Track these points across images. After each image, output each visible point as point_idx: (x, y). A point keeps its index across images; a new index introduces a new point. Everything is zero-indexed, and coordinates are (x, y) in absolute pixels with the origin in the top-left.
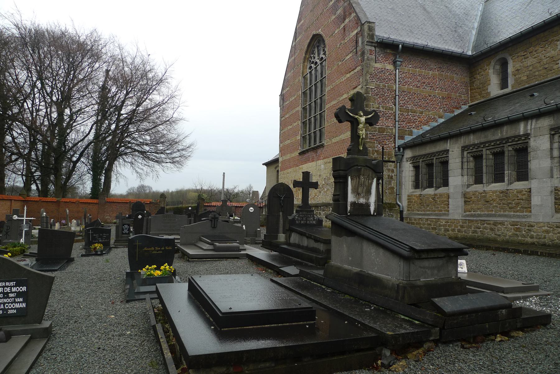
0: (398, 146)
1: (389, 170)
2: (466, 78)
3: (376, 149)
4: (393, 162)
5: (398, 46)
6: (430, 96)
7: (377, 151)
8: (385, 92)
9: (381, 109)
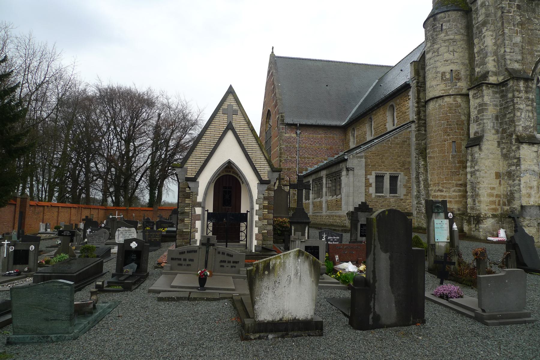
3: (286, 179)
5: (297, 124)
8: (291, 149)
9: (289, 158)
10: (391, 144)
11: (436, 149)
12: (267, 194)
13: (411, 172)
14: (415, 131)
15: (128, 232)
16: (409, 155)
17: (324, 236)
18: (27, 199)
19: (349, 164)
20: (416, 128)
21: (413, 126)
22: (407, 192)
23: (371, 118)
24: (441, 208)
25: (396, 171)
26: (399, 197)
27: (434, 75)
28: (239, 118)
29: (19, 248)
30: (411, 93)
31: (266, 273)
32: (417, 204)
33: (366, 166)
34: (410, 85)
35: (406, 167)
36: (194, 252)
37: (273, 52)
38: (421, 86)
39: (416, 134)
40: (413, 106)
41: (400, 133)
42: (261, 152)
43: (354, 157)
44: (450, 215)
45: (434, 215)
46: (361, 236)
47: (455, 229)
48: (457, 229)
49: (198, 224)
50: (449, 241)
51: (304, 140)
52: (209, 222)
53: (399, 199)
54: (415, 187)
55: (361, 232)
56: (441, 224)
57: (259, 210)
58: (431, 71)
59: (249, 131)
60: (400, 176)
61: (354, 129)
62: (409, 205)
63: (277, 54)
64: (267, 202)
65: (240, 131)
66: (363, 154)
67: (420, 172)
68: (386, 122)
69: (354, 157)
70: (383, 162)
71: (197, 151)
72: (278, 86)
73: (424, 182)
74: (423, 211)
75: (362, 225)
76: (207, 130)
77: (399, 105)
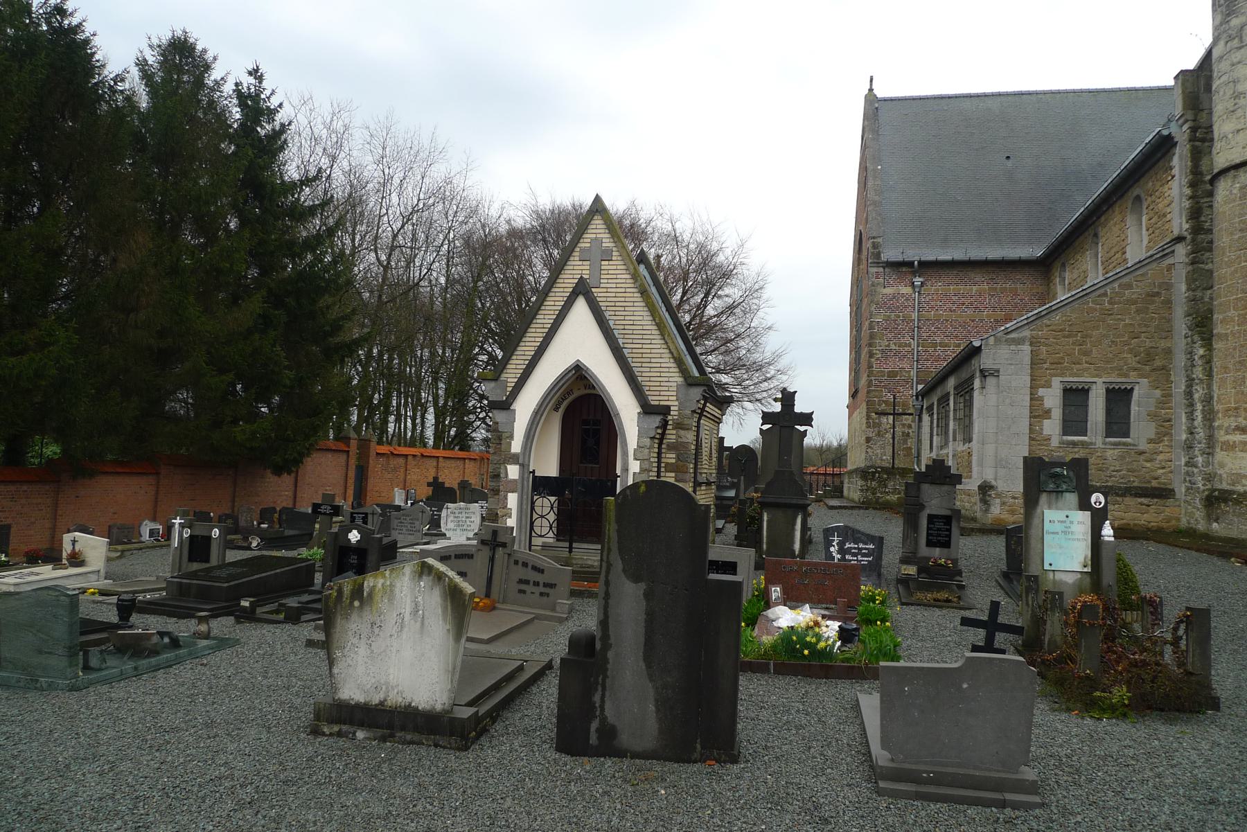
0: (917, 393)
1: (904, 425)
2: (1040, 287)
3: (884, 399)
4: (912, 414)
5: (913, 262)
6: (973, 321)
7: (886, 402)
8: (898, 325)
9: (893, 347)
10: (1110, 303)
11: (1233, 312)
12: (674, 437)
13: (1172, 378)
14: (1186, 264)
15: (464, 511)
16: (1168, 332)
17: (836, 540)
18: (370, 441)
19: (986, 360)
20: (1188, 255)
21: (1181, 251)
22: (1157, 433)
23: (1096, 235)
24: (1065, 480)
25: (1126, 376)
26: (1134, 445)
27: (1230, 105)
28: (615, 267)
29: (197, 533)
30: (1176, 161)
31: (356, 603)
32: (1187, 464)
33: (1035, 362)
34: (1173, 138)
35: (1158, 363)
36: (469, 558)
37: (871, 90)
38: (1202, 137)
39: (1189, 272)
40: (1181, 194)
41: (1139, 272)
42: (663, 342)
43: (998, 341)
44: (1097, 499)
45: (1044, 498)
46: (930, 544)
47: (1107, 539)
48: (1112, 539)
49: (512, 500)
50: (1088, 569)
51: (933, 300)
52: (535, 497)
53: (1133, 452)
54: (1184, 420)
55: (928, 535)
56: (1065, 522)
57: (639, 473)
58: (1221, 93)
59: (636, 295)
60: (1137, 388)
61: (1063, 265)
62: (1164, 468)
63: (880, 93)
64: (674, 456)
65: (618, 295)
66: (1026, 333)
67: (1194, 376)
68: (1124, 244)
69: (998, 341)
70: (1086, 353)
71: (527, 344)
72: (875, 170)
73: (1204, 407)
74: (1200, 485)
75: (931, 518)
76: (548, 299)
77: (1151, 195)
